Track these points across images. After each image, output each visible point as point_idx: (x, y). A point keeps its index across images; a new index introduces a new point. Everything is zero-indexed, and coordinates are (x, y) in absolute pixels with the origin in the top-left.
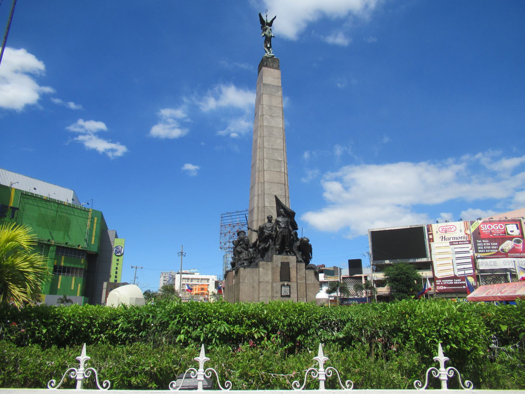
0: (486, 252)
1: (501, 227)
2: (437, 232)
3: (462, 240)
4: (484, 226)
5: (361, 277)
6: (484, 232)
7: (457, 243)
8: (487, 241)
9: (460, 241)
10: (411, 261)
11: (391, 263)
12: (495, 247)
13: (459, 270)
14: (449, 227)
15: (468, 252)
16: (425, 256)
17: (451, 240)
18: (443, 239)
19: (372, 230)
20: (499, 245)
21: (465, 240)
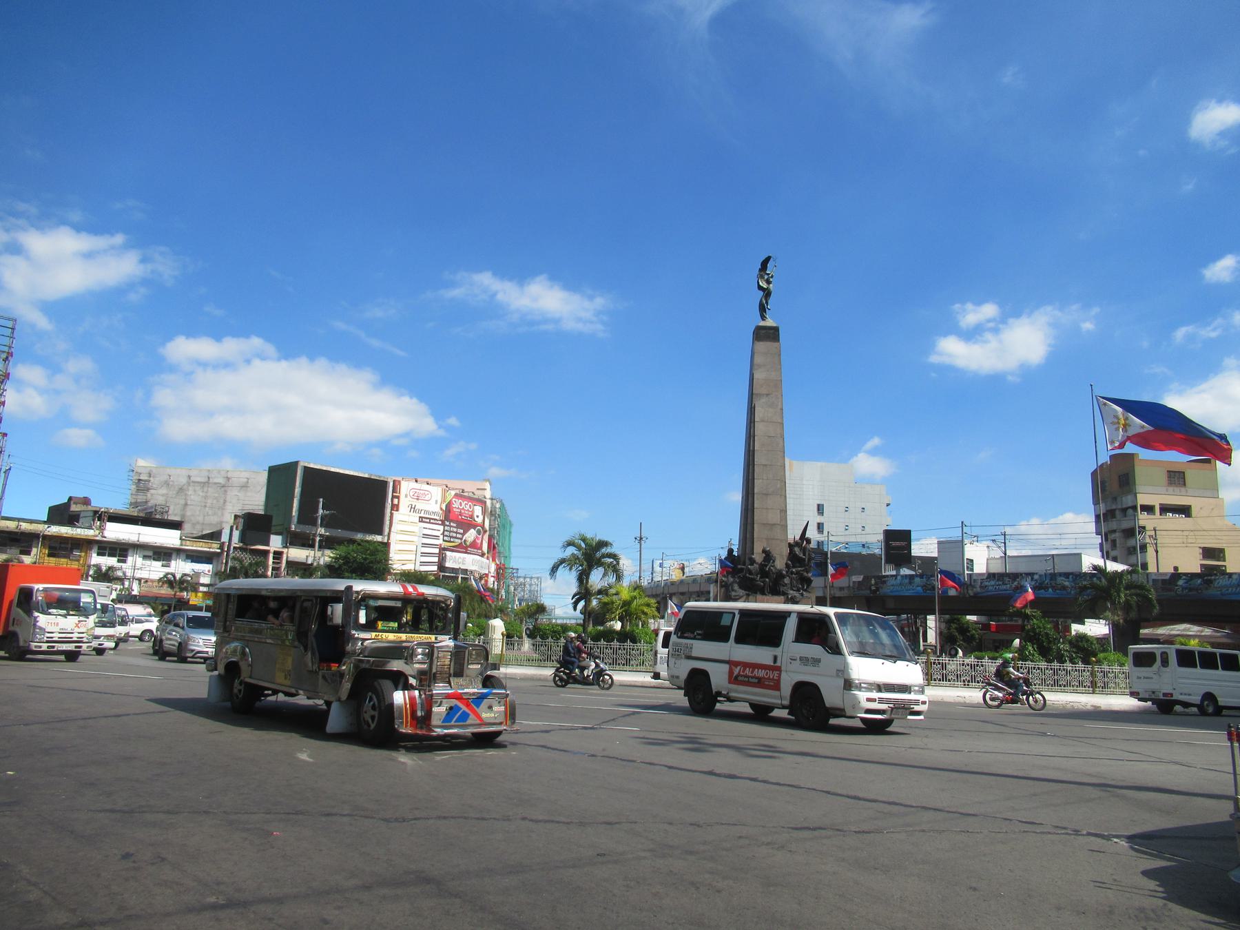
0: (450, 542)
1: (470, 507)
2: (406, 496)
3: (435, 517)
4: (455, 502)
5: (266, 553)
6: (455, 510)
7: (428, 520)
8: (455, 525)
9: (432, 519)
10: (359, 536)
11: (327, 534)
12: (459, 536)
13: (423, 563)
14: (423, 492)
15: (436, 537)
16: (380, 533)
17: (422, 515)
18: (412, 510)
19: (307, 465)
20: (463, 534)
21: (438, 518)
